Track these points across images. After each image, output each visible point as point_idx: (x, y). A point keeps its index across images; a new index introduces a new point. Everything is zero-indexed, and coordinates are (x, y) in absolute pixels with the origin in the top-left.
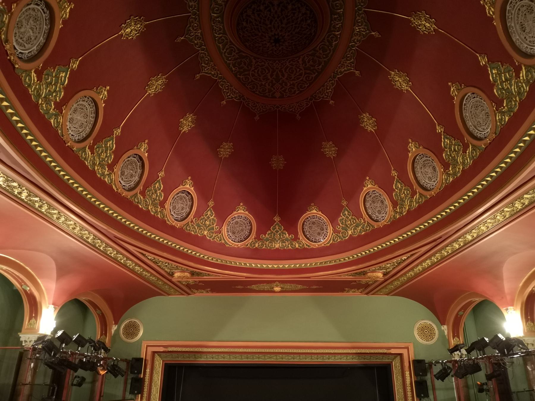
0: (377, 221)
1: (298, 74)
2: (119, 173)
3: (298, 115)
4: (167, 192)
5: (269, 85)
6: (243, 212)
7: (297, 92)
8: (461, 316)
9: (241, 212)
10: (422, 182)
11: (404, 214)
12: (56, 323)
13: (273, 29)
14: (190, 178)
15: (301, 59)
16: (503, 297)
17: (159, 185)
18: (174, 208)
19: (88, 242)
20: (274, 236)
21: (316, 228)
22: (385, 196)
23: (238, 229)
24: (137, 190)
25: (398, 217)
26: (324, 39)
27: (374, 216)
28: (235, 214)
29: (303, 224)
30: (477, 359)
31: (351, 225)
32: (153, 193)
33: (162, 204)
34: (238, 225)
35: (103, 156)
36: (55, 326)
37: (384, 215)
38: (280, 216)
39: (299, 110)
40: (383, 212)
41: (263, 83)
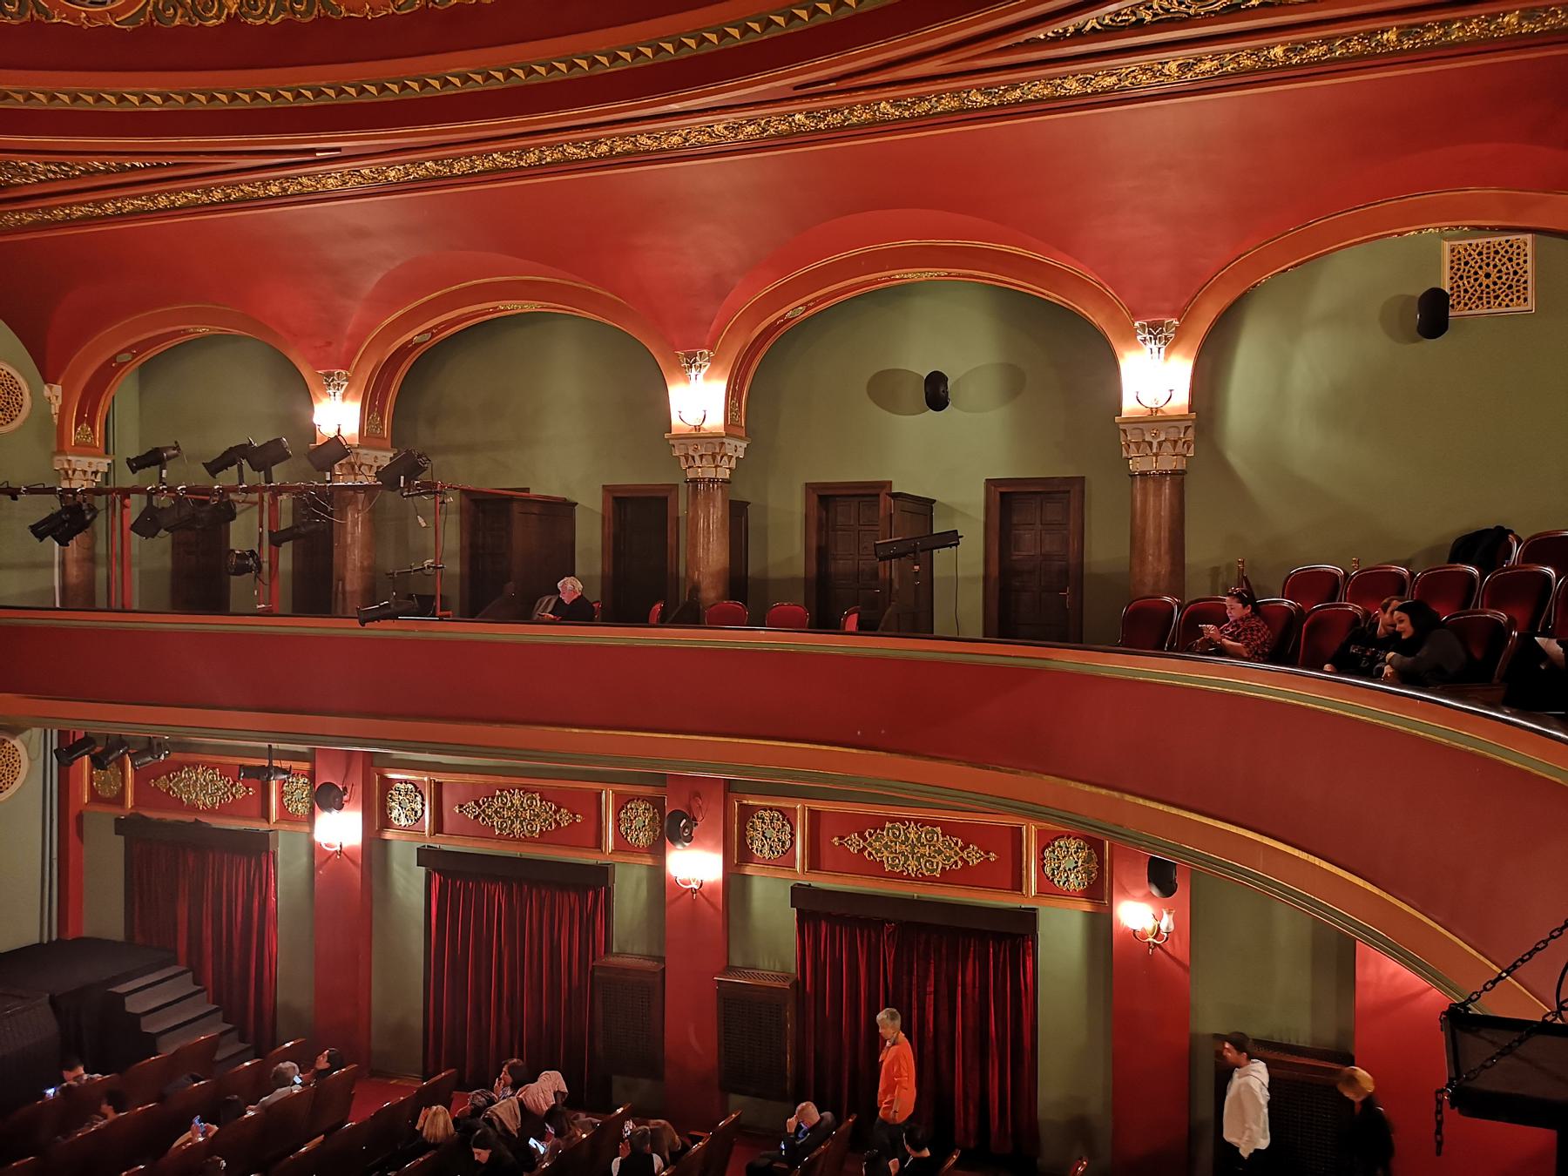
8: (123, 365)
16: (329, 344)
25: (177, 22)
30: (235, 490)
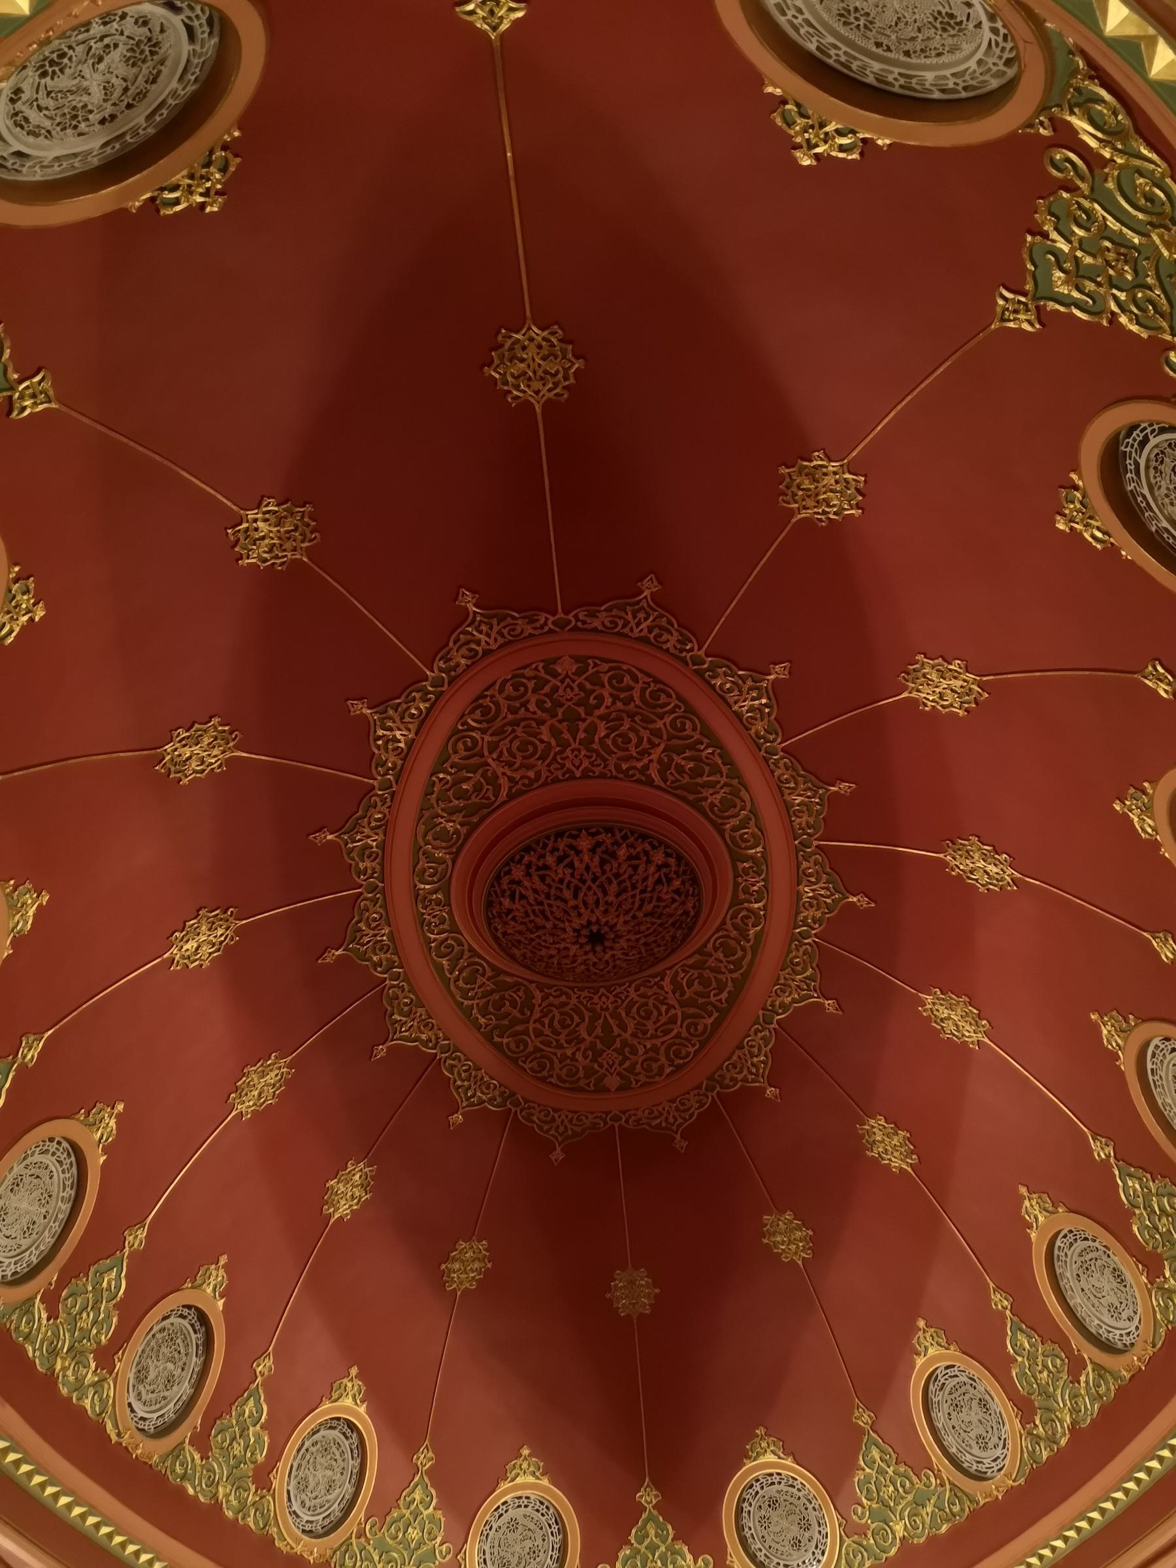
0: (980, 1477)
1: (664, 1019)
2: (131, 1375)
3: (678, 1137)
4: (280, 1429)
5: (586, 1057)
6: (531, 1479)
7: (668, 1070)
9: (527, 1482)
10: (1093, 1325)
11: (1063, 1442)
13: (582, 910)
14: (354, 1371)
15: (667, 980)
18: (303, 1486)
21: (785, 1524)
22: (987, 1383)
23: (517, 1548)
24: (185, 1432)
25: (1045, 1455)
26: (724, 923)
27: (967, 1460)
28: (505, 1492)
29: (739, 1510)
32: (233, 1439)
33: (263, 1477)
34: (517, 1535)
37: (998, 1452)
38: (657, 1484)
39: (680, 1121)
40: (995, 1440)
41: (569, 1053)
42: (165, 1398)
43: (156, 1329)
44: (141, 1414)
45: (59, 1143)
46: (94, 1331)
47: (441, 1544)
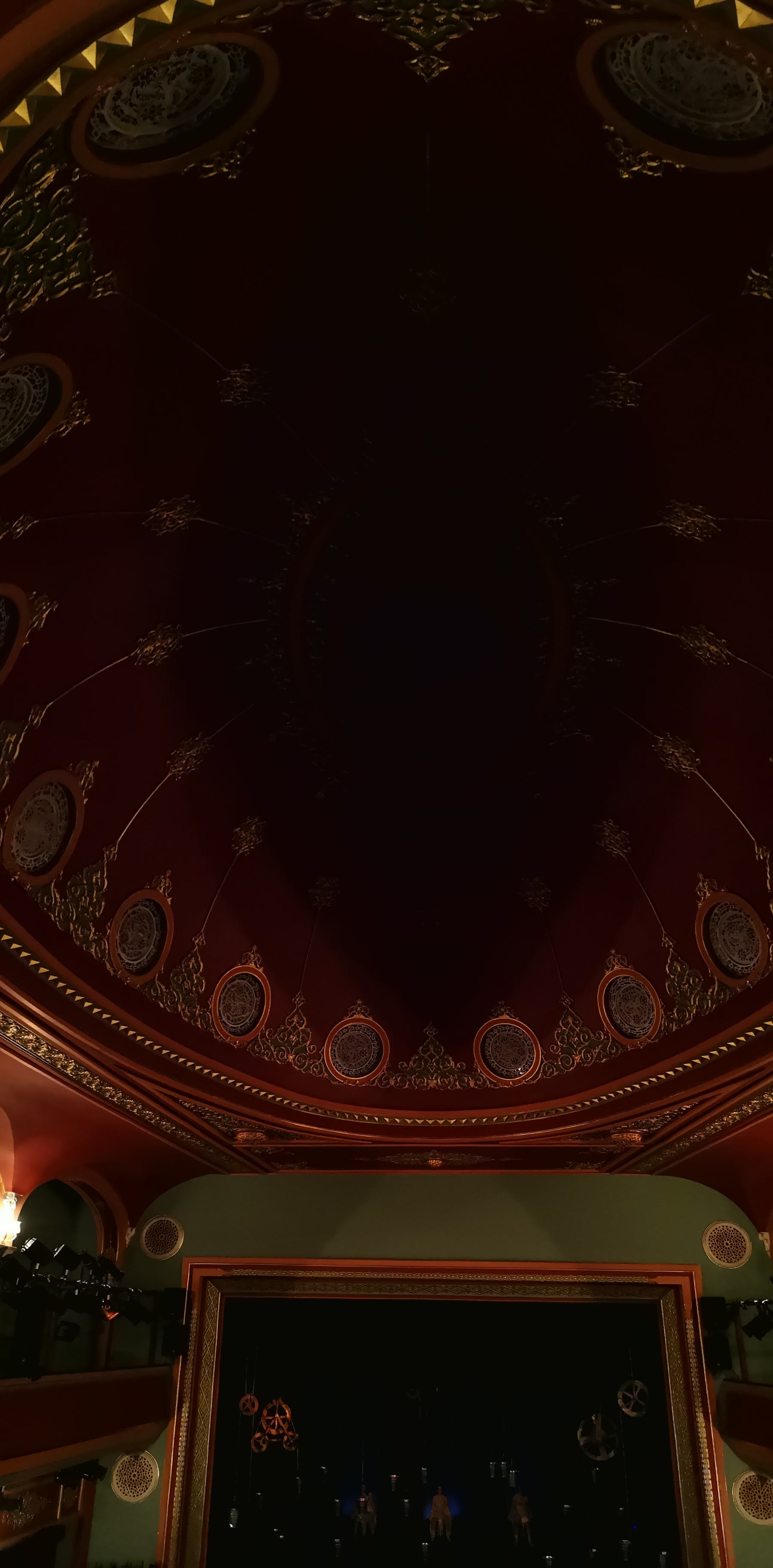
2: (117, 938)
4: (212, 976)
9: (358, 1020)
12: (21, 1225)
14: (255, 948)
17: (196, 964)
18: (227, 1008)
19: (66, 1075)
20: (426, 1064)
24: (155, 973)
28: (347, 1023)
29: (484, 1042)
31: (579, 1043)
32: (184, 980)
33: (204, 1000)
35: (85, 901)
36: (18, 1230)
42: (140, 953)
43: (130, 911)
44: (127, 961)
45: (56, 787)
46: (91, 909)
47: (310, 1045)
